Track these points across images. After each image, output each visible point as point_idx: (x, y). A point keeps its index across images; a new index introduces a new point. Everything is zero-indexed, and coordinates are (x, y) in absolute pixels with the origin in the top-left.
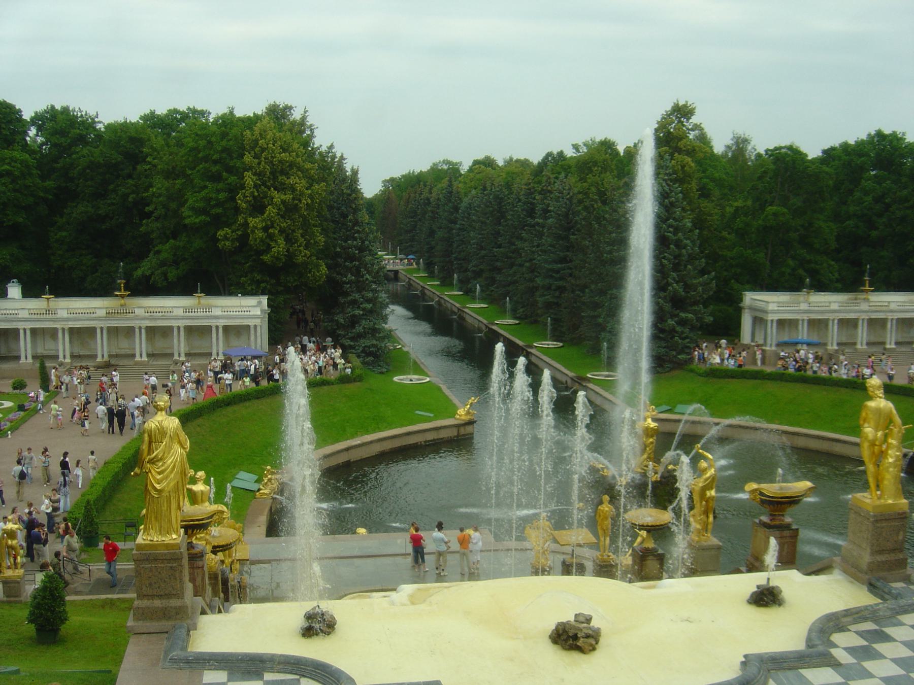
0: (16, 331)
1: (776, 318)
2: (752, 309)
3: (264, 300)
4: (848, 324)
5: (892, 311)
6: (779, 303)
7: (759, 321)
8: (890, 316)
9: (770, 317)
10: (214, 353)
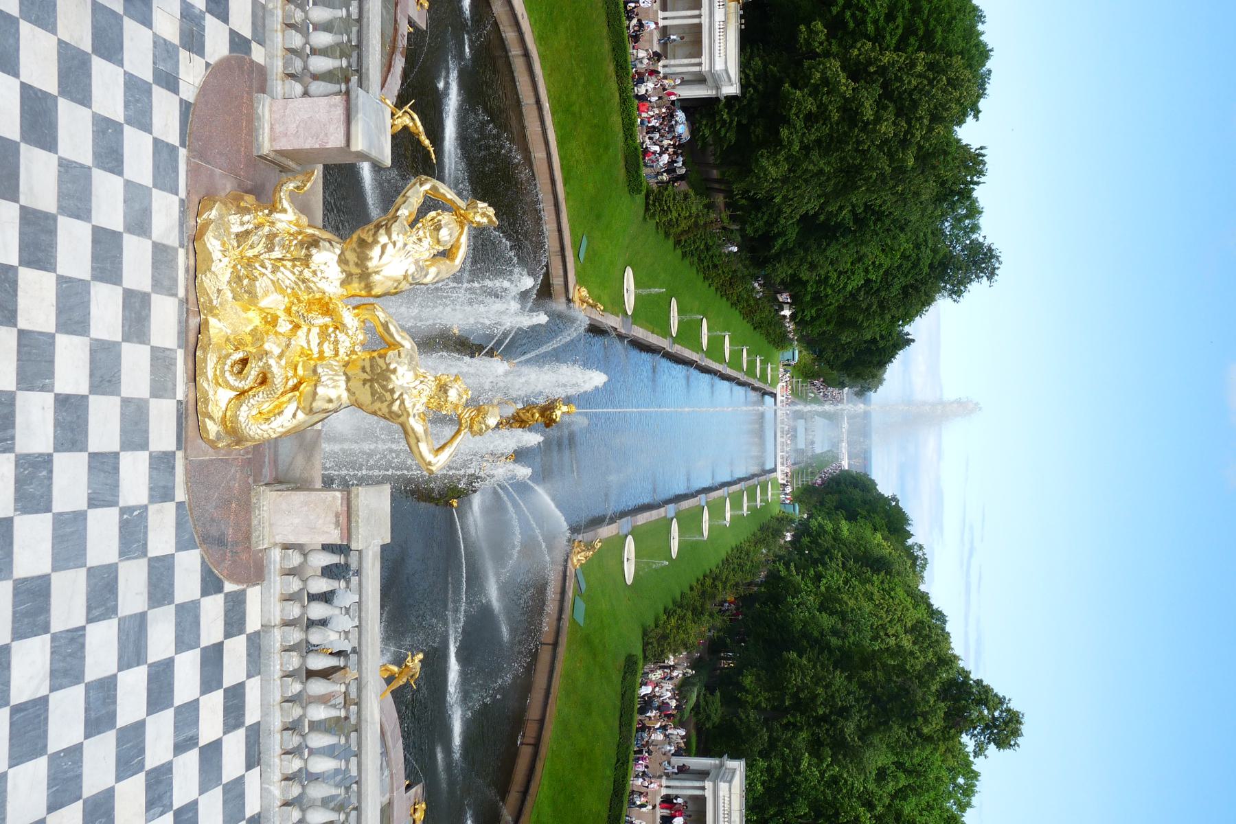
1: (709, 794)
2: (722, 765)
3: (731, 89)
6: (730, 814)
7: (703, 775)
9: (708, 785)
10: (667, 14)
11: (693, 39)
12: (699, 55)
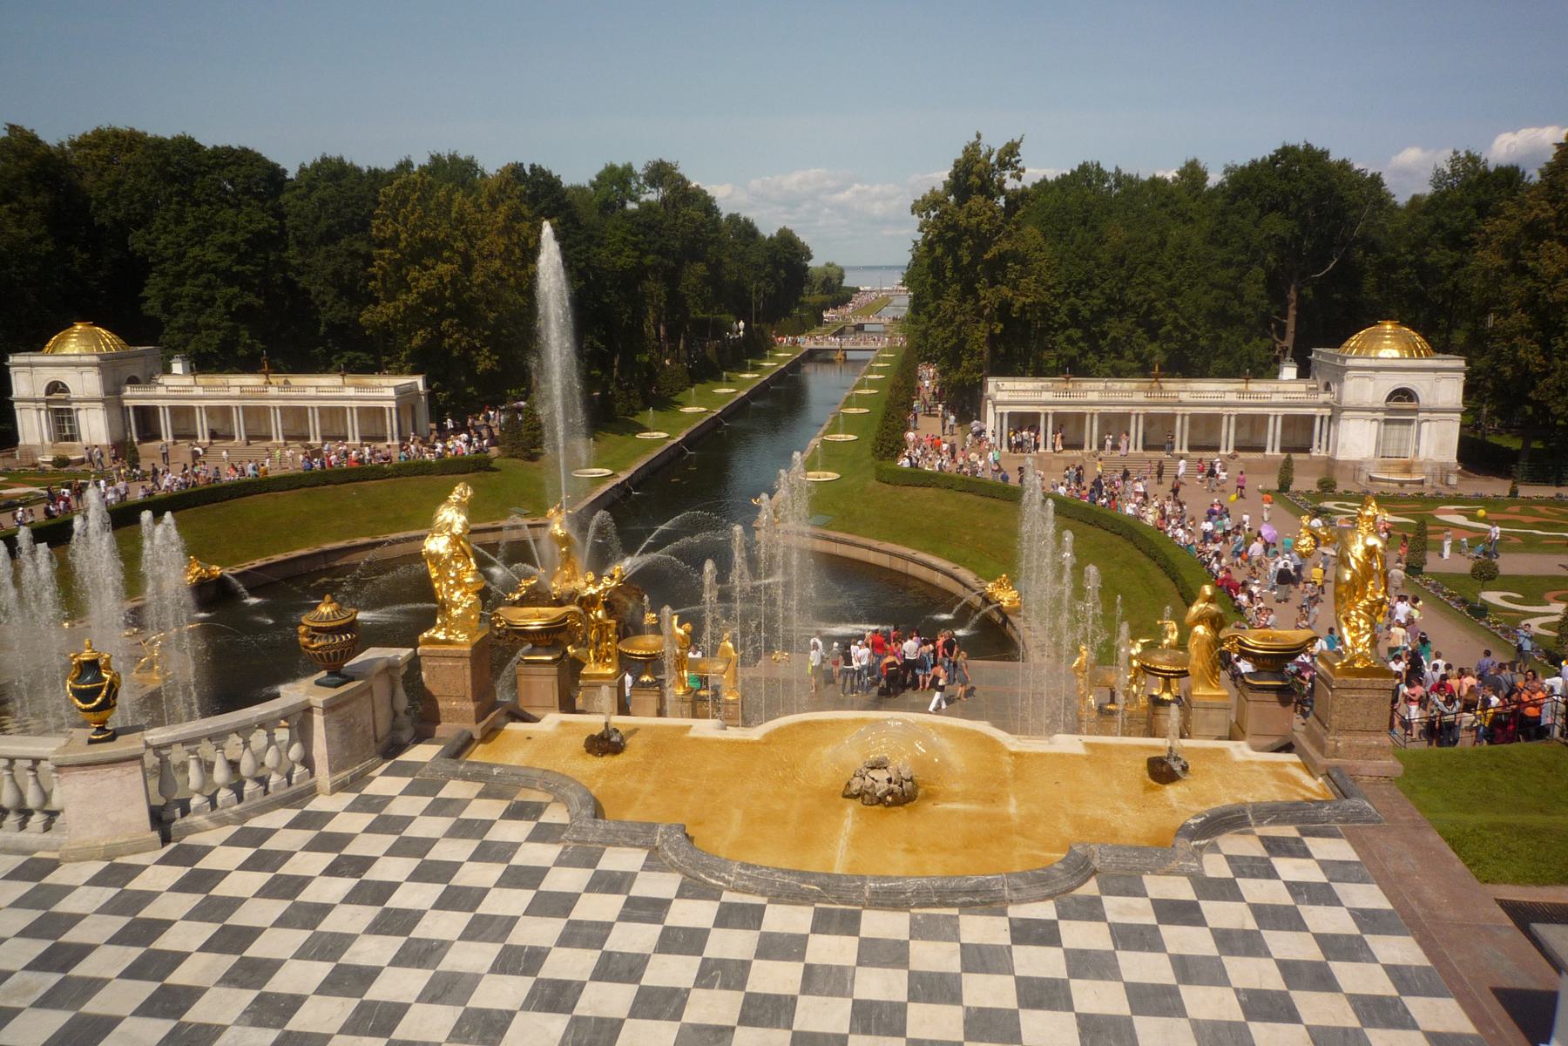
0: (155, 409)
1: (1007, 409)
3: (419, 381)
4: (1114, 424)
5: (1181, 404)
8: (1179, 410)
11: (372, 416)
12: (382, 409)
